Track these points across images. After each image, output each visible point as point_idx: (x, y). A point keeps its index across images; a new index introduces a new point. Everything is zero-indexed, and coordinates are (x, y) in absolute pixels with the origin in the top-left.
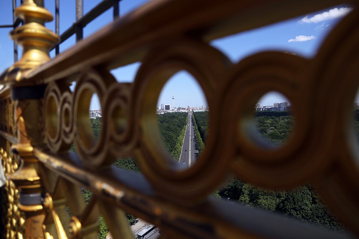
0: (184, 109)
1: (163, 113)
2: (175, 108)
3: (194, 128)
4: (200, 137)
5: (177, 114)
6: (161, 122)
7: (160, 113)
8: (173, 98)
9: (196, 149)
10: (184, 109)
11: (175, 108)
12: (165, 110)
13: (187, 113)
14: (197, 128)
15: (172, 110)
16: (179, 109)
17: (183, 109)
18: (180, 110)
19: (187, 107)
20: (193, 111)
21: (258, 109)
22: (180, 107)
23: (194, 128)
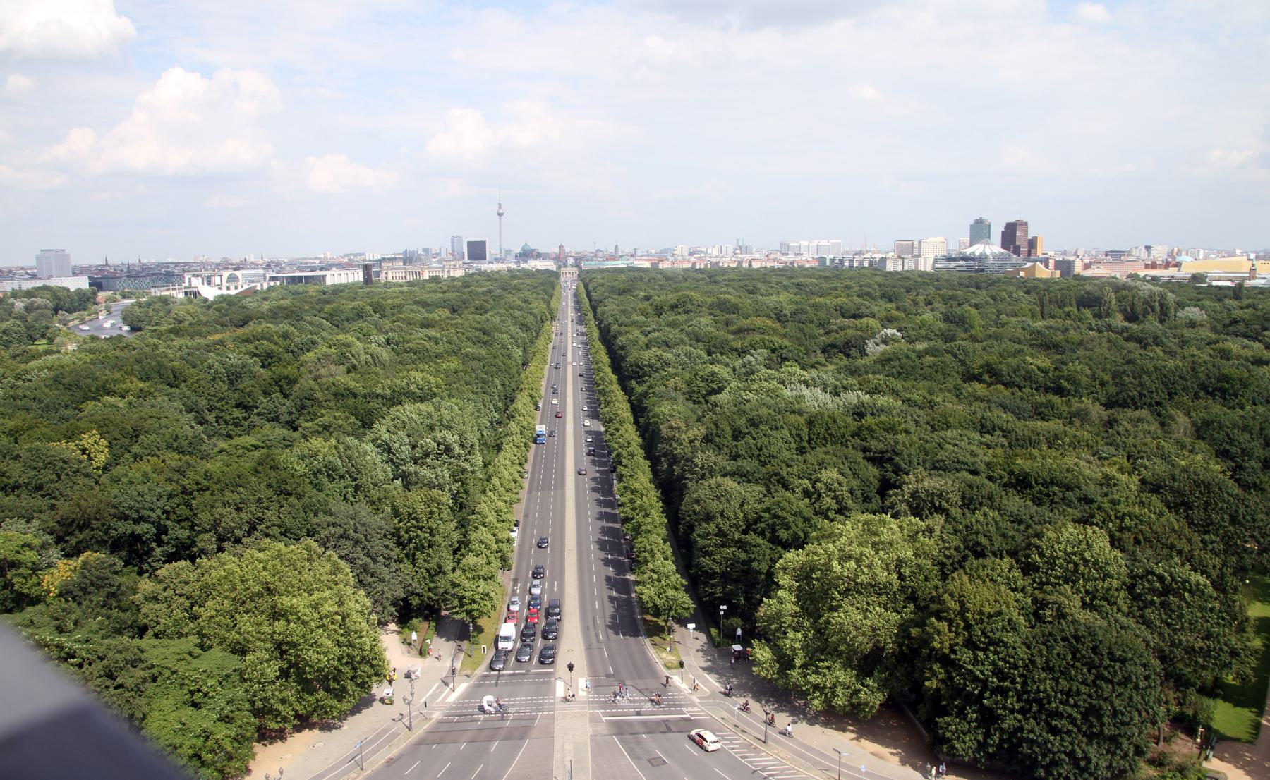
1: (459, 273)
3: (583, 334)
4: (608, 370)
5: (514, 277)
6: (454, 311)
9: (594, 415)
11: (508, 252)
12: (466, 260)
13: (556, 275)
14: (596, 334)
21: (832, 261)
23: (583, 334)
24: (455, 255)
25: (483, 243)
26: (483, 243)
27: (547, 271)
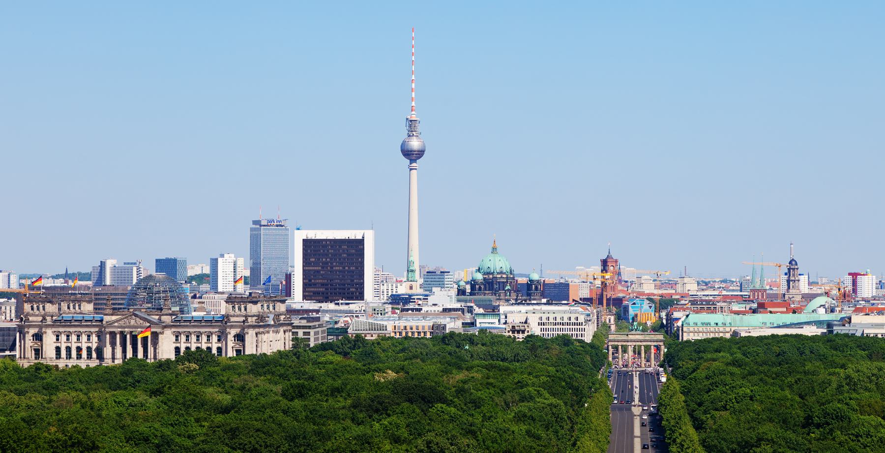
0: (557, 293)
1: (273, 343)
2: (434, 278)
7: (240, 338)
8: (415, 144)
10: (557, 293)
11: (434, 278)
12: (297, 299)
15: (396, 300)
16: (490, 288)
17: (529, 292)
18: (493, 310)
19: (583, 277)
20: (667, 328)
22: (499, 264)
24: (265, 287)
25: (354, 249)
26: (354, 249)
27: (565, 341)
